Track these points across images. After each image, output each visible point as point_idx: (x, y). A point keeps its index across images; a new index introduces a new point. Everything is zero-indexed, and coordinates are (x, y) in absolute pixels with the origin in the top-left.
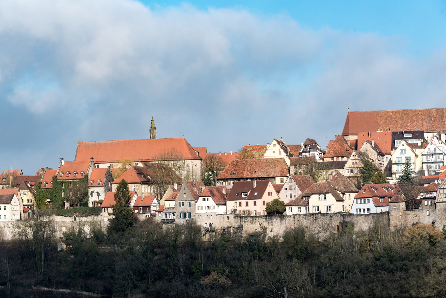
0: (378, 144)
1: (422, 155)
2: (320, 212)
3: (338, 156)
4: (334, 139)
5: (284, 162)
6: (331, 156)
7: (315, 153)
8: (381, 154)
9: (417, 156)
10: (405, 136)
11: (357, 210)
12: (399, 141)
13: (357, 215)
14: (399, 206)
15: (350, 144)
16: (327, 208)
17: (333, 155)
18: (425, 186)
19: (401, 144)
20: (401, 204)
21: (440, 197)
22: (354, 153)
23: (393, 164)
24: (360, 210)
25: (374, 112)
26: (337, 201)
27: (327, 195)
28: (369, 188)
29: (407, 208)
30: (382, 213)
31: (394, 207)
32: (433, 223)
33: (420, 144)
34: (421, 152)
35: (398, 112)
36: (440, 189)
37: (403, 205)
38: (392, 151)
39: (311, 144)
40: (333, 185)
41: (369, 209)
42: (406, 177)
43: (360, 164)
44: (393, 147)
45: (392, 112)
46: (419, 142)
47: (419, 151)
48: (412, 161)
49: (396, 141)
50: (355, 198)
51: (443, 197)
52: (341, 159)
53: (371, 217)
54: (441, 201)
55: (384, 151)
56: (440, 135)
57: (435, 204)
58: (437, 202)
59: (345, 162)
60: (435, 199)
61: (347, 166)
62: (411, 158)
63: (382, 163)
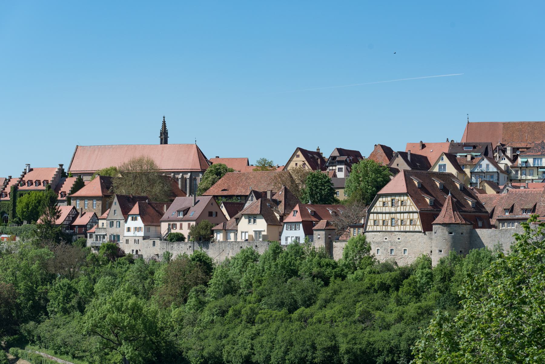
21: (369, 224)
31: (319, 236)
51: (372, 224)
54: (370, 230)
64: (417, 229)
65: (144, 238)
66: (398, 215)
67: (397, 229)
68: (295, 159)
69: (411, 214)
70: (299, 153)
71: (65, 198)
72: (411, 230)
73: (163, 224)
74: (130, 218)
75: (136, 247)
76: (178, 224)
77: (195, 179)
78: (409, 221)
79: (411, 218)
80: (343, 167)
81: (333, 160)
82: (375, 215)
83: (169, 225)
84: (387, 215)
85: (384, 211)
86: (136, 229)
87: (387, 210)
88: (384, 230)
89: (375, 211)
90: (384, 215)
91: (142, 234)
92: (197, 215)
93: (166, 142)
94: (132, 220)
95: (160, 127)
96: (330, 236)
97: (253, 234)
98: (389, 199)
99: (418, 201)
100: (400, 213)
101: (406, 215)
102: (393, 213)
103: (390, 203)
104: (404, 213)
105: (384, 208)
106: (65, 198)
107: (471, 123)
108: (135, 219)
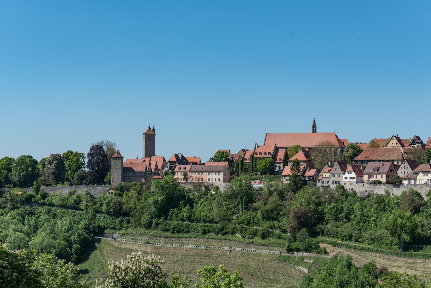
5: (400, 150)
39: (417, 140)
65: (357, 182)
68: (392, 141)
70: (394, 138)
71: (281, 161)
73: (364, 176)
74: (347, 173)
75: (351, 187)
76: (375, 176)
77: (337, 151)
80: (420, 145)
81: (413, 142)
83: (369, 176)
86: (351, 178)
91: (355, 180)
92: (386, 171)
93: (316, 132)
94: (348, 173)
95: (312, 124)
97: (427, 181)
106: (281, 161)
108: (350, 172)
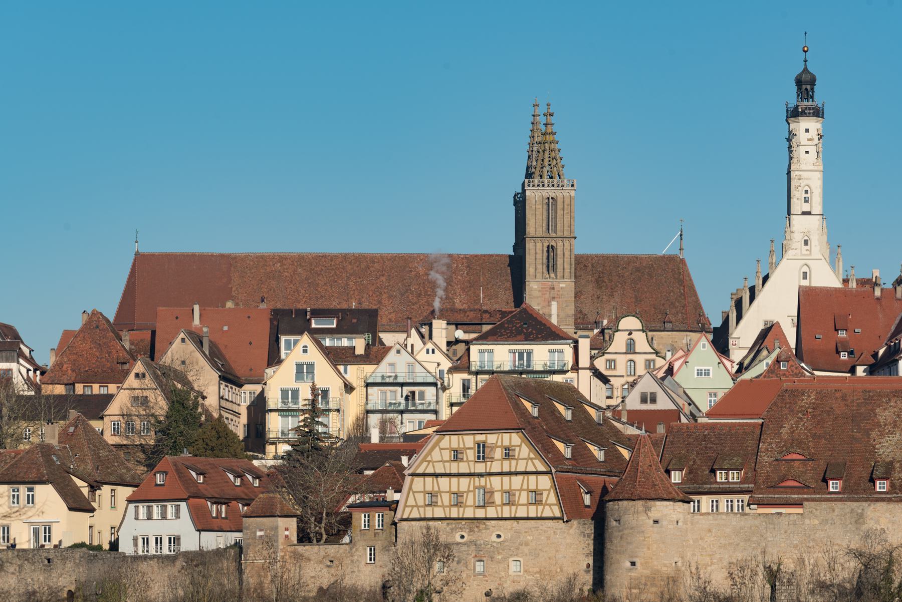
0: (222, 347)
1: (368, 385)
2: (13, 546)
3: (87, 380)
4: (76, 324)
6: (65, 379)
7: (14, 366)
8: (229, 378)
9: (349, 388)
10: (314, 326)
11: (135, 540)
12: (292, 338)
13: (136, 558)
14: (276, 528)
15: (132, 343)
16: (36, 533)
17: (70, 376)
18: (368, 473)
19: (299, 350)
20: (281, 522)
21: (411, 502)
22: (139, 367)
23: (271, 411)
24: (146, 541)
25: (222, 256)
26: (71, 509)
27: (38, 488)
28: (178, 471)
29: (304, 537)
30: (219, 553)
31: (259, 533)
32: (385, 587)
33: (360, 350)
34: (362, 376)
35: (301, 259)
36: (413, 475)
37: (288, 528)
38: (270, 371)
40: (58, 457)
41: (175, 540)
42: (309, 445)
43: (160, 405)
44: (274, 359)
45: (282, 259)
46: (359, 344)
47: (355, 373)
48: (332, 406)
49: (283, 339)
50: (130, 501)
52: (96, 389)
53: (180, 563)
54: (415, 515)
55: (240, 371)
56: (430, 325)
57: (395, 524)
58: (403, 520)
59: (108, 399)
60: (395, 511)
61: (113, 409)
62: (331, 395)
63: (235, 408)
64: (547, 513)
66: (496, 481)
67: (491, 512)
69: (532, 478)
72: (532, 514)
78: (524, 494)
79: (532, 487)
82: (429, 480)
84: (464, 481)
85: (454, 471)
87: (463, 468)
88: (454, 515)
89: (430, 470)
90: (454, 480)
96: (287, 533)
98: (469, 440)
99: (545, 450)
100: (501, 474)
101: (517, 481)
102: (481, 475)
103: (471, 455)
104: (510, 474)
105: (454, 465)
107: (143, 255)
